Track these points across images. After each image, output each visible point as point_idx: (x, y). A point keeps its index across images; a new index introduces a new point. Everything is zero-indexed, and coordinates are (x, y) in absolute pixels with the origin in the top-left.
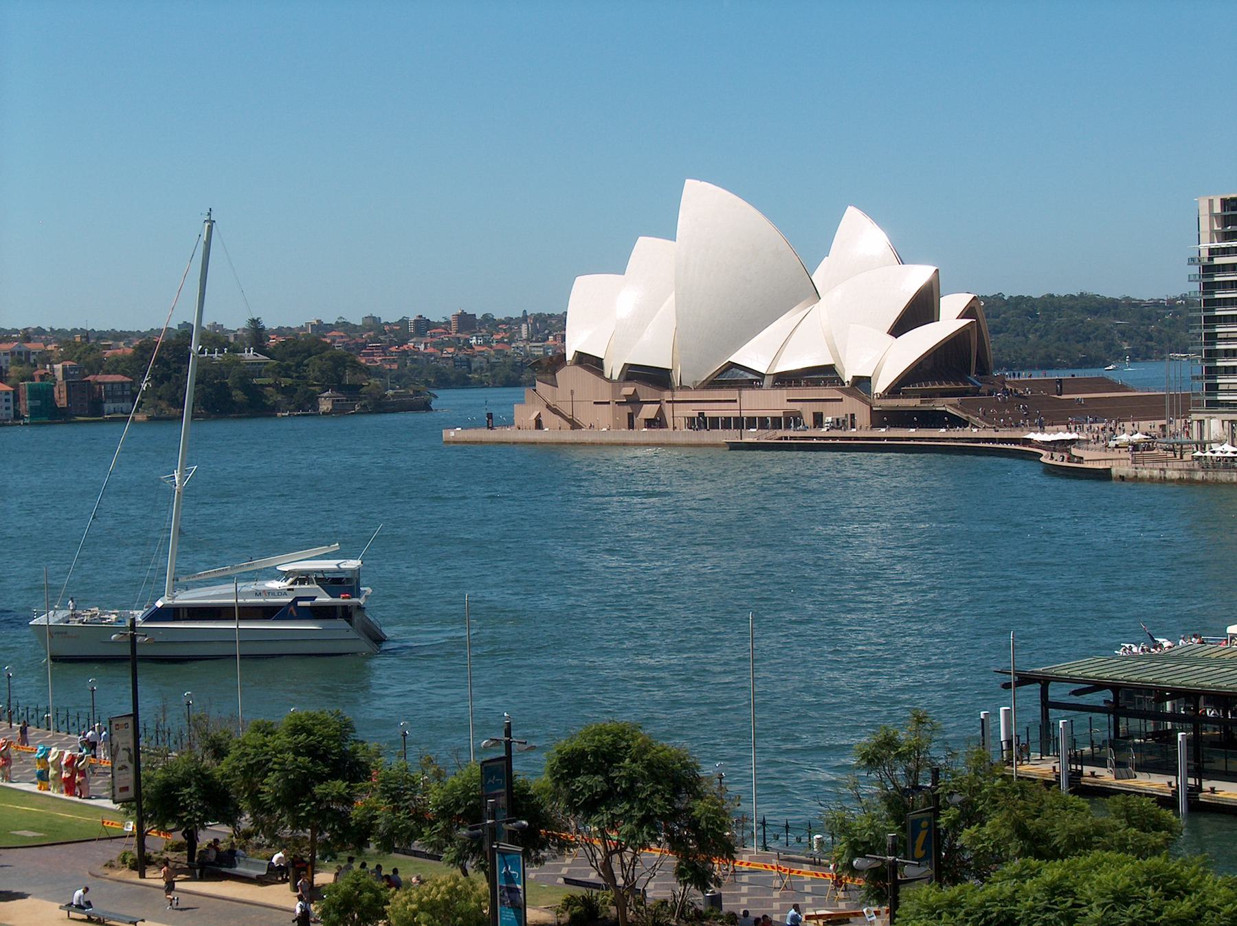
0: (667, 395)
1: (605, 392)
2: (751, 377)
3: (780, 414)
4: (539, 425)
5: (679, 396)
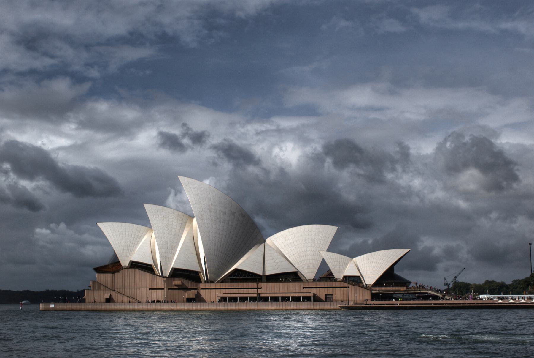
0: (201, 286)
1: (160, 282)
3: (311, 295)
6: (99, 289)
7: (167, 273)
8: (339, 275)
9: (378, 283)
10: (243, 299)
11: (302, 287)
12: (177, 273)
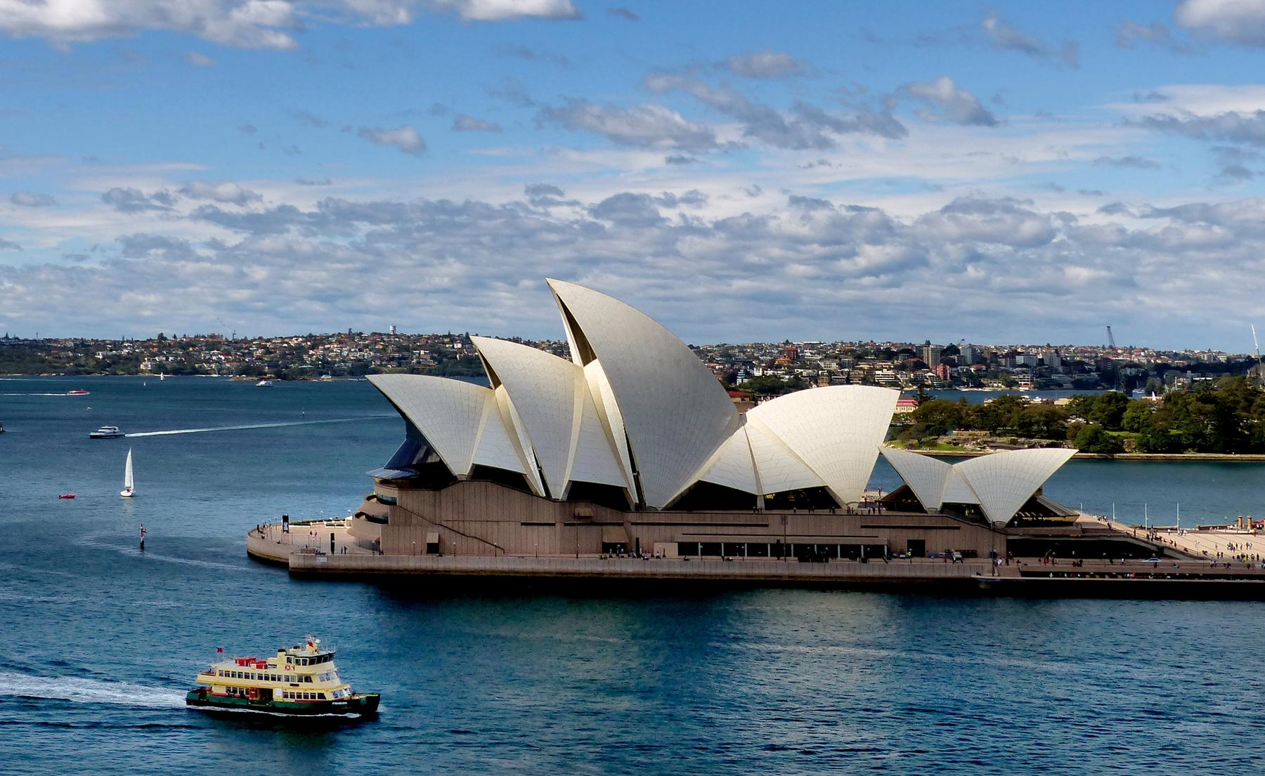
0: (633, 517)
6: (407, 523)
7: (559, 492)
8: (931, 500)
9: (1018, 521)
10: (733, 549)
11: (859, 524)
12: (579, 491)
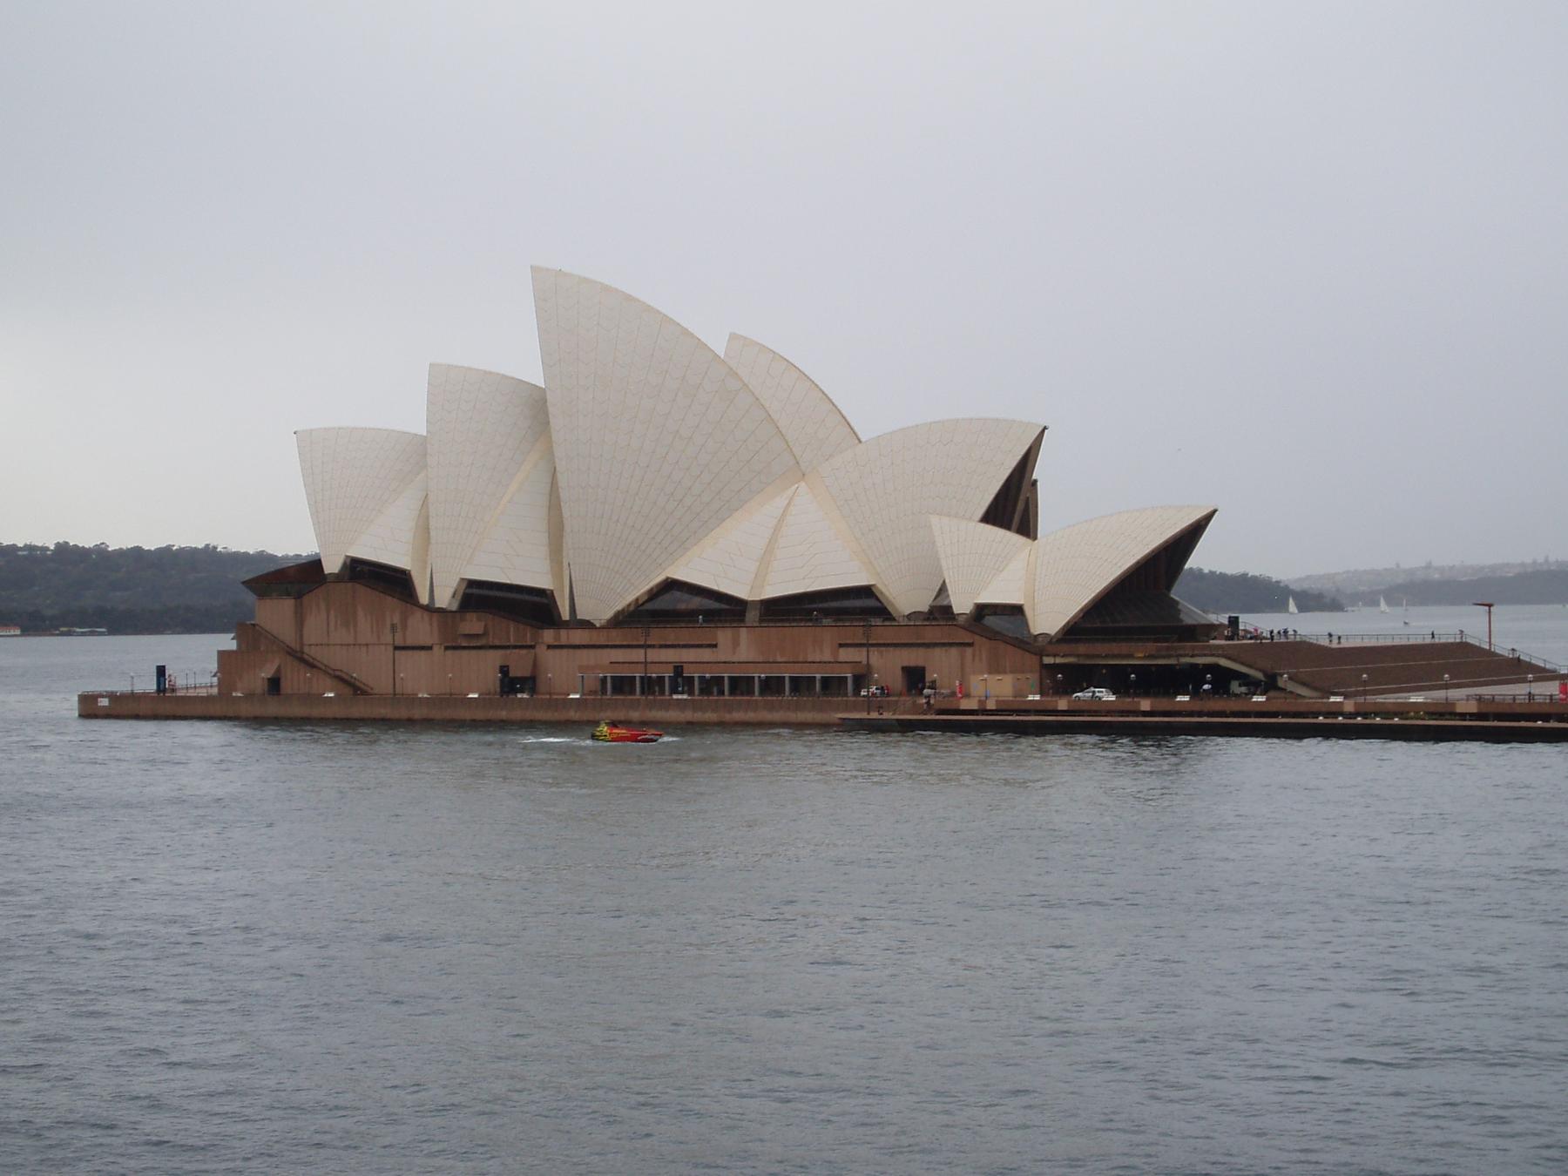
0: (548, 635)
1: (421, 629)
2: (716, 605)
4: (274, 684)
5: (578, 636)
8: (962, 604)
9: (1074, 631)
